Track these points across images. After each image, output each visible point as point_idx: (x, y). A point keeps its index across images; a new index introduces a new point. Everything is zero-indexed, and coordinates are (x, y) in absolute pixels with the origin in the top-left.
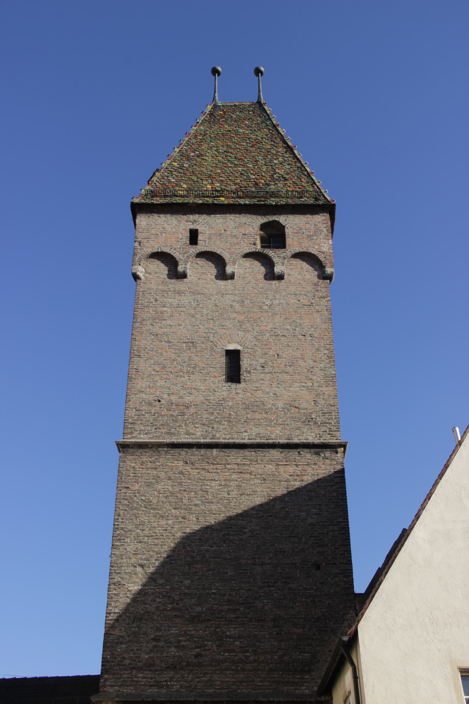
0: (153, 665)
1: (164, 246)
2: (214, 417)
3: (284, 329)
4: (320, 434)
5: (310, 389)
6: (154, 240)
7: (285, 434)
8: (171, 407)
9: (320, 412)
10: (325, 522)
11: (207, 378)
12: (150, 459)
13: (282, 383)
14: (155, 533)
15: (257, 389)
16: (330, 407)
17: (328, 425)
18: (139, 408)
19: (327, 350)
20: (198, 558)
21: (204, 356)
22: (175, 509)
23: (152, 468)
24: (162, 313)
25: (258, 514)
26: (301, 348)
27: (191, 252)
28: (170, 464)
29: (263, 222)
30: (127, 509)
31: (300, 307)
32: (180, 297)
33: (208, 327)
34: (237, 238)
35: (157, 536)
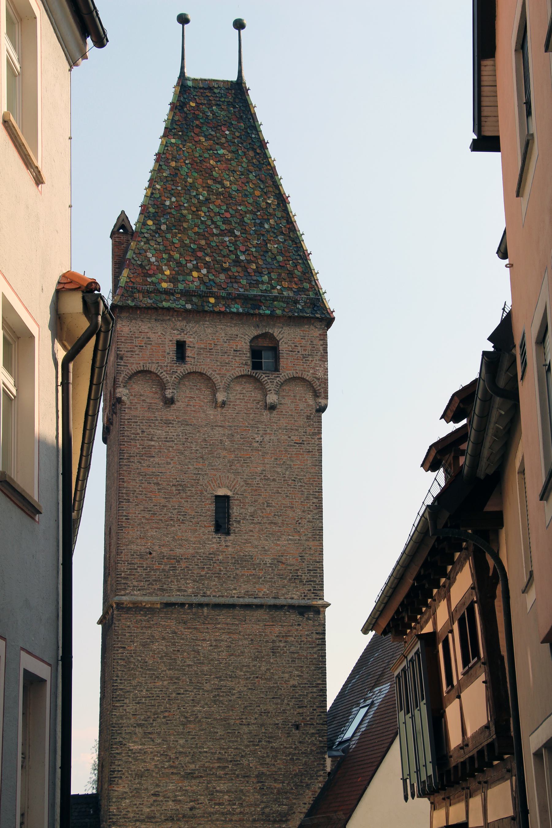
0: (154, 817)
1: (149, 363)
2: (204, 573)
3: (274, 471)
4: (304, 593)
5: (297, 543)
6: (138, 354)
7: (272, 592)
8: (163, 560)
9: (306, 569)
10: (305, 684)
11: (198, 528)
12: (144, 618)
13: (270, 535)
14: (151, 693)
15: (247, 541)
16: (316, 564)
17: (312, 583)
18: (131, 561)
19: (315, 498)
20: (192, 719)
21: (194, 502)
22: (170, 669)
23: (145, 627)
24: (150, 447)
25: (245, 675)
26: (291, 495)
27: (179, 372)
28: (164, 623)
29: (256, 334)
30: (125, 670)
31: (291, 446)
32: (168, 428)
33: (197, 467)
34: (228, 355)
35: (153, 697)
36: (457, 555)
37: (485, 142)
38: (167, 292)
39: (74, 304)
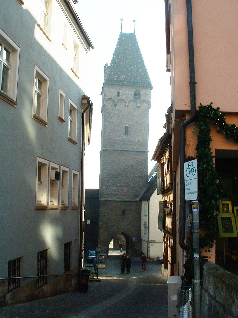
36: (167, 148)
37: (168, 70)
38: (115, 81)
39: (85, 102)
